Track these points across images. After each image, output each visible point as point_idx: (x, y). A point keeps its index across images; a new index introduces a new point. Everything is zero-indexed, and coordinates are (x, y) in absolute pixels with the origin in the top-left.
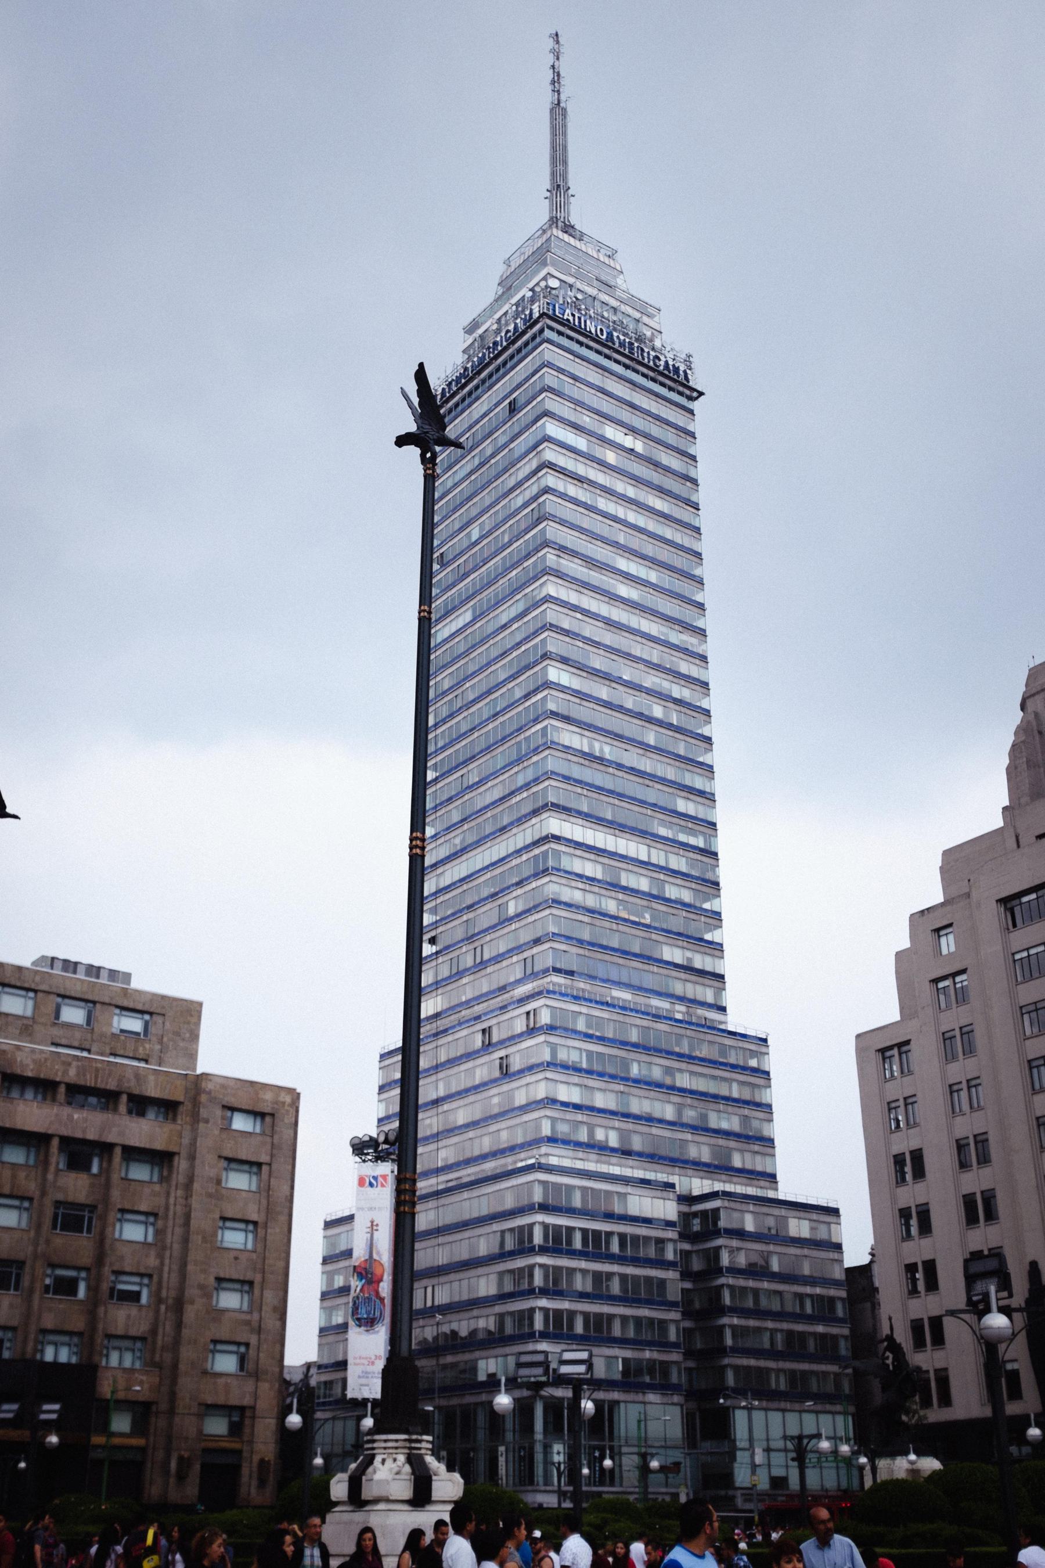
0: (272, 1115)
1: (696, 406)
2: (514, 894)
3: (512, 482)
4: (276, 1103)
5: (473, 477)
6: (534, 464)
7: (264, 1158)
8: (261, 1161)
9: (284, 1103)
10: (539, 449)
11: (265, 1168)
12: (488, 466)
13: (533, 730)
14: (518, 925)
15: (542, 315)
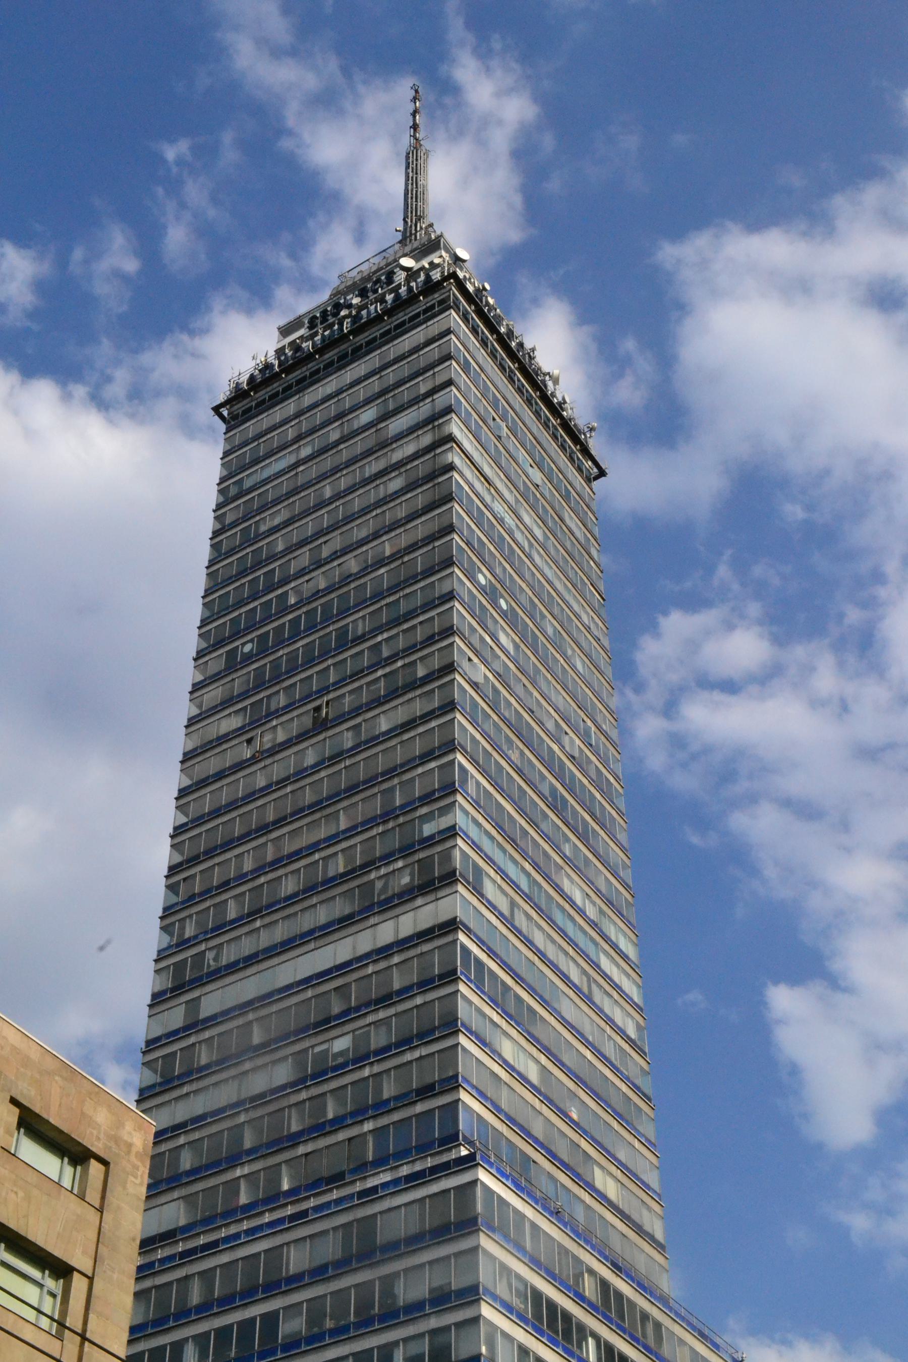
0: (105, 1163)
1: (596, 484)
2: (370, 1019)
3: (381, 465)
4: (117, 1140)
5: (301, 468)
6: (426, 440)
7: (79, 1259)
8: (74, 1263)
9: (130, 1146)
10: (436, 423)
11: (79, 1284)
12: (334, 451)
13: (420, 770)
14: (377, 1069)
15: (445, 279)
